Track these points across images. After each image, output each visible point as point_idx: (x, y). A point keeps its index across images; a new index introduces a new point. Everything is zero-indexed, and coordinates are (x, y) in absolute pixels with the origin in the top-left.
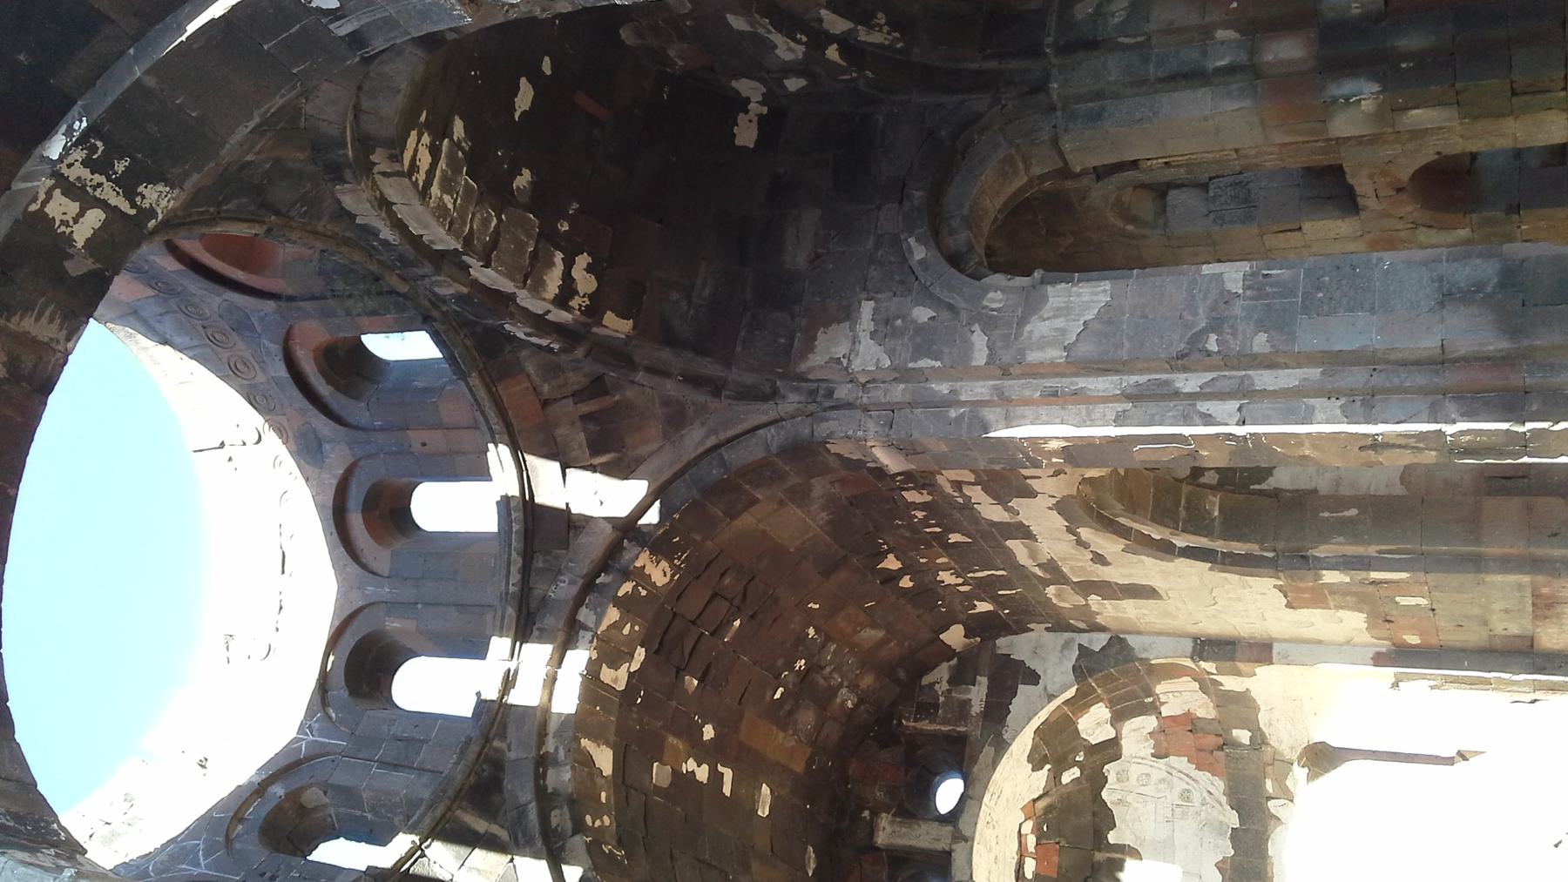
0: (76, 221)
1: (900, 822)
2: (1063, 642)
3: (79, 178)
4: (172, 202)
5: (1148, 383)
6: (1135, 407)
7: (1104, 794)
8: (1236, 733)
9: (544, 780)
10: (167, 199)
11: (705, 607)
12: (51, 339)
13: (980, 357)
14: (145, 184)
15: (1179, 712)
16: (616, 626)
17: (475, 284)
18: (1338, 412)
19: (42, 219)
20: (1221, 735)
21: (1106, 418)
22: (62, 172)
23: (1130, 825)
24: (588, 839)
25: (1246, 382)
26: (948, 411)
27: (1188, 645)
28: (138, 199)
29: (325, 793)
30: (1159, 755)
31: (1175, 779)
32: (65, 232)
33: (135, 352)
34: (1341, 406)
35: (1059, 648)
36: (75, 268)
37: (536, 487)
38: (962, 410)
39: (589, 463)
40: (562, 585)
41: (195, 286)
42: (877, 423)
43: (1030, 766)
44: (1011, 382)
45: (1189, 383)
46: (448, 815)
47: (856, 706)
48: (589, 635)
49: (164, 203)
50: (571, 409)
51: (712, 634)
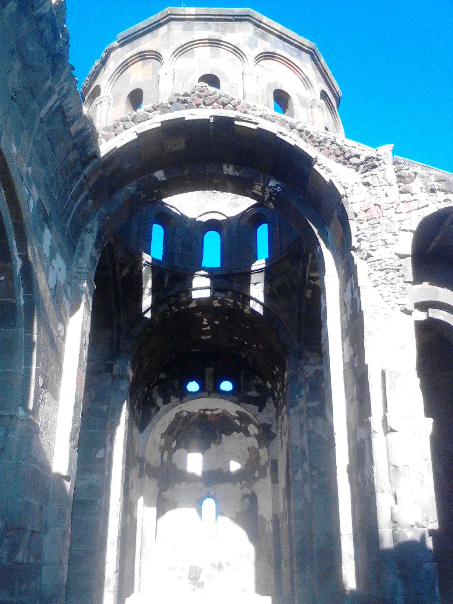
0: (257, 190)
7: (235, 433)
9: (182, 293)
13: (310, 405)
16: (229, 302)
17: (308, 255)
19: (254, 185)
24: (168, 309)
27: (275, 458)
30: (248, 448)
40: (237, 285)
43: (236, 411)
44: (305, 413)
45: (306, 466)
47: (243, 357)
48: (224, 296)
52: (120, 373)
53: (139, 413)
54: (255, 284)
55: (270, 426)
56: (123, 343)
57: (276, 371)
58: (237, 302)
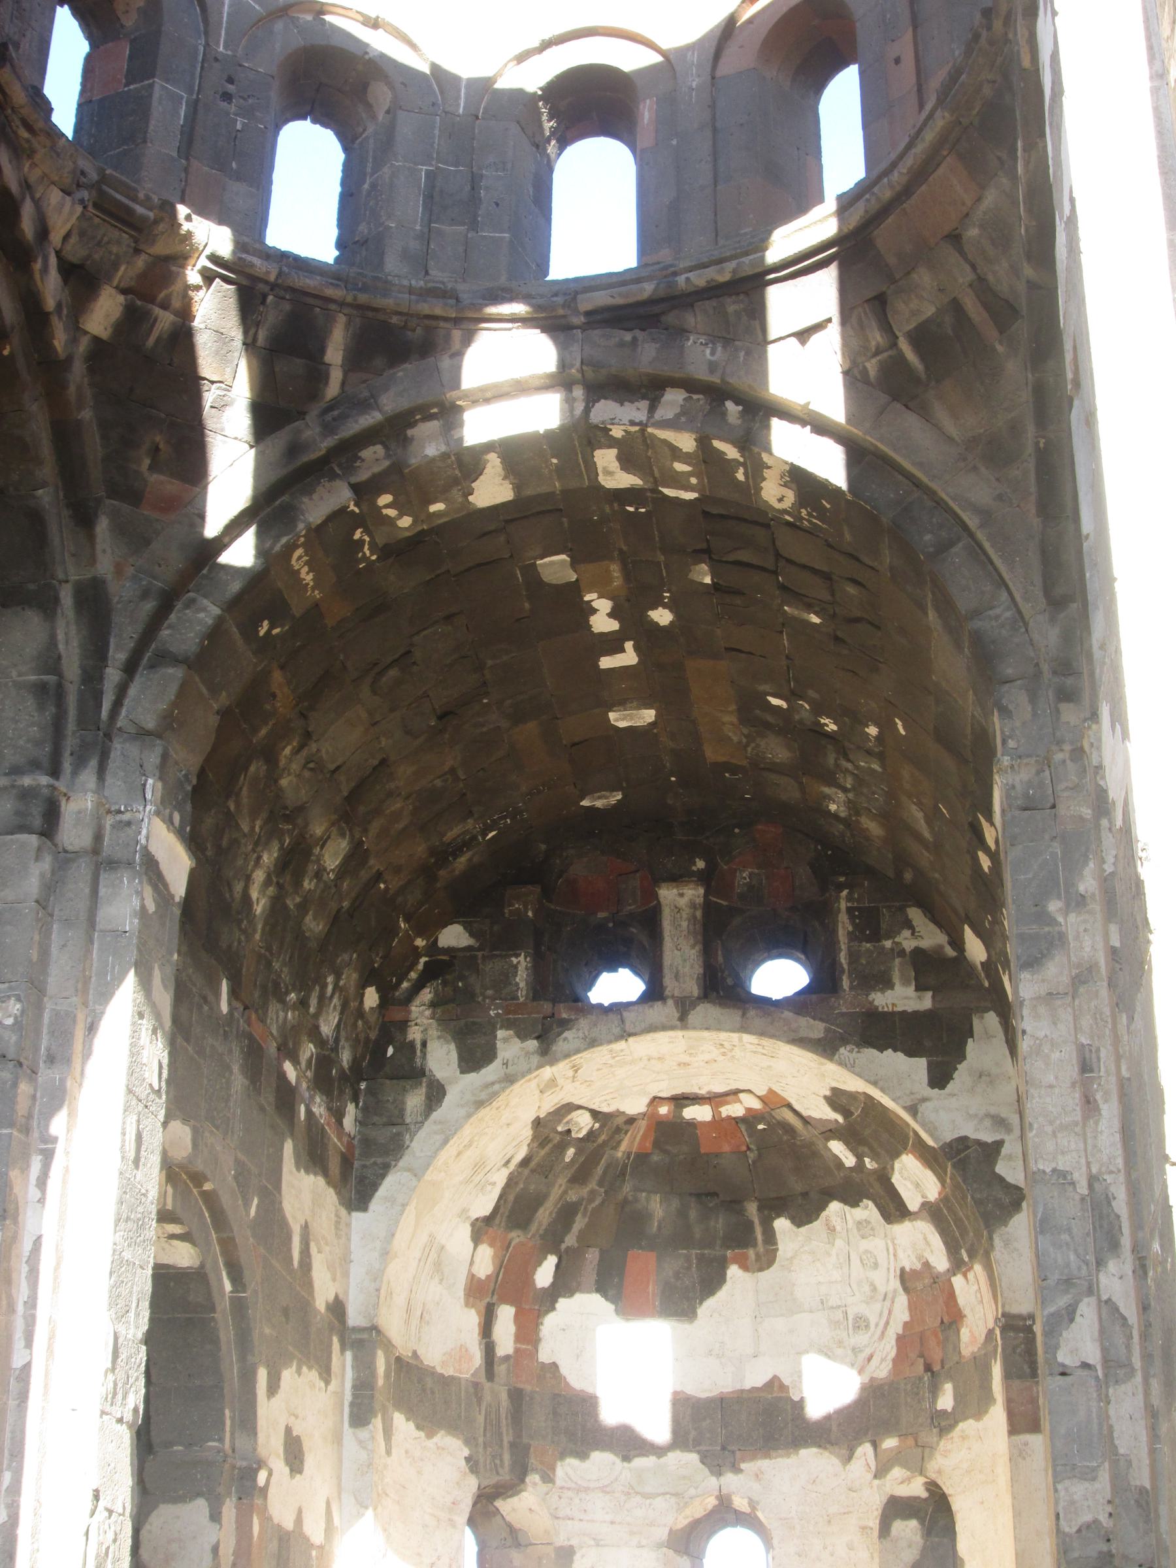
1: (695, 917)
2: (1003, 1115)
5: (1113, 1216)
6: (1083, 1199)
7: (835, 1207)
8: (949, 1388)
11: (804, 567)
15: (961, 1301)
16: (676, 453)
18: (1087, 1518)
20: (943, 1367)
21: (1060, 1157)
23: (806, 1248)
24: (352, 507)
25: (1121, 1372)
26: (1059, 898)
29: (388, 112)
30: (905, 1278)
31: (877, 1306)
34: (1096, 1521)
35: (993, 1110)
38: (1061, 919)
39: (897, 333)
40: (708, 351)
42: (1029, 784)
43: (828, 1093)
44: (1104, 992)
46: (333, 307)
47: (835, 816)
48: (641, 416)
50: (961, 280)
51: (783, 587)
52: (98, 837)
53: (339, 1115)
54: (803, 335)
55: (992, 1151)
56: (122, 691)
57: (987, 850)
58: (717, 444)
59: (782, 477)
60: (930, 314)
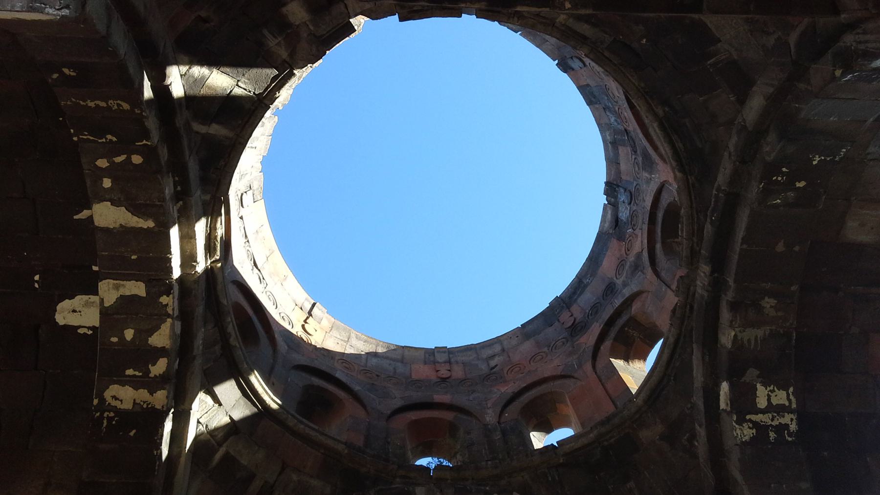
0: (768, 395)
3: (783, 417)
4: (736, 435)
10: (739, 435)
12: (744, 331)
14: (755, 434)
22: (792, 415)
24: (144, 142)
28: (751, 425)
32: (770, 387)
33: (379, 342)
36: (752, 373)
37: (246, 403)
39: (225, 445)
41: (417, 396)
49: (739, 432)
59: (144, 402)
60: (242, 462)
